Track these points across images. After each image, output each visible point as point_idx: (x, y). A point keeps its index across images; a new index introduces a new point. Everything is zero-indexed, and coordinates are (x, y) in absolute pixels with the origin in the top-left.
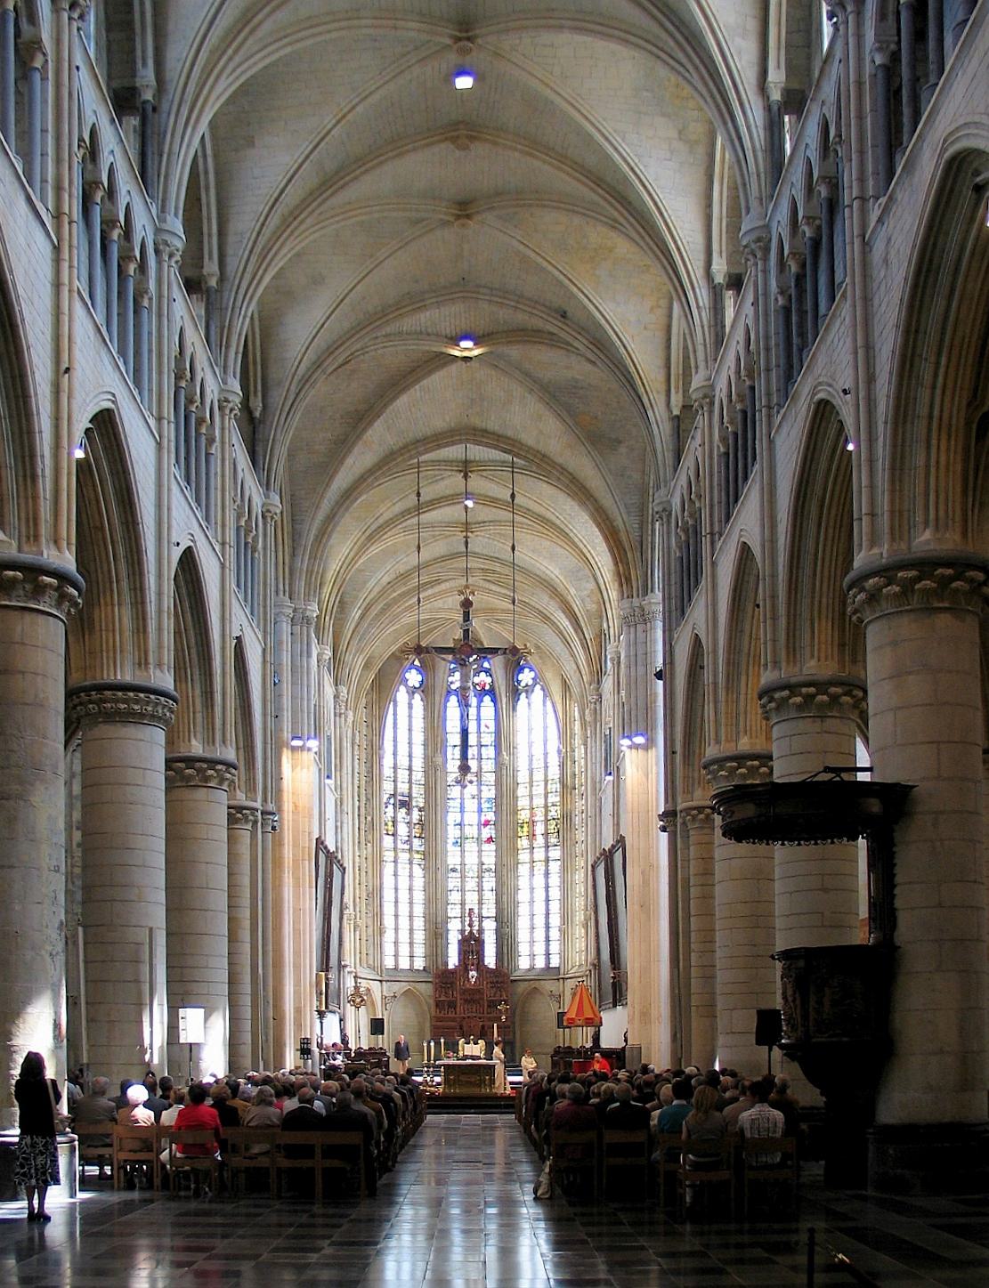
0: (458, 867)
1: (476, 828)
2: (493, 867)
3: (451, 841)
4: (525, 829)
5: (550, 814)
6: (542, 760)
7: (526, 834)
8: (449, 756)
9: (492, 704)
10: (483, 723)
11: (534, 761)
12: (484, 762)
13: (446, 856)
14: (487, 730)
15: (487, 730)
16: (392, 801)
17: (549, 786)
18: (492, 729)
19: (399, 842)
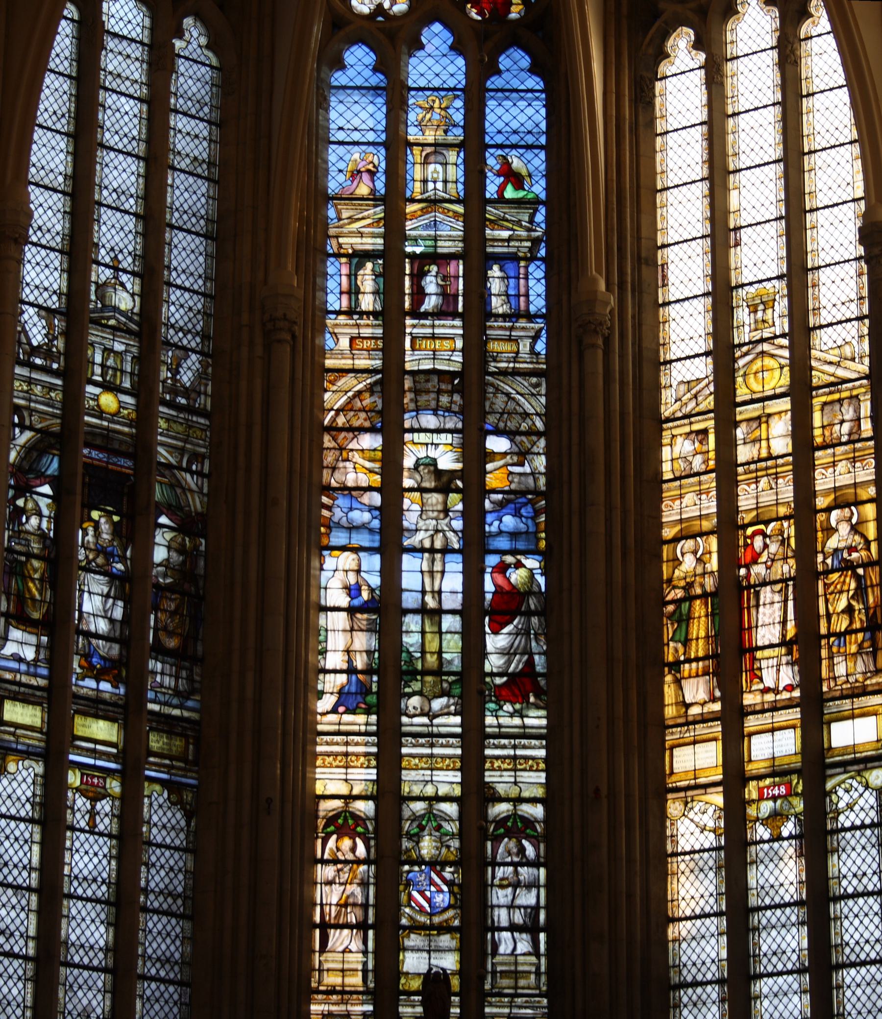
0: (365, 808)
1: (450, 622)
2: (537, 811)
3: (332, 683)
4: (699, 628)
5: (833, 543)
6: (782, 305)
7: (699, 648)
8: (334, 302)
9: (534, 82)
10: (492, 162)
11: (742, 315)
12: (496, 330)
13: (308, 759)
14: (510, 193)
15: (510, 193)
16: (53, 467)
17: (817, 419)
18: (539, 189)
19: (76, 663)
